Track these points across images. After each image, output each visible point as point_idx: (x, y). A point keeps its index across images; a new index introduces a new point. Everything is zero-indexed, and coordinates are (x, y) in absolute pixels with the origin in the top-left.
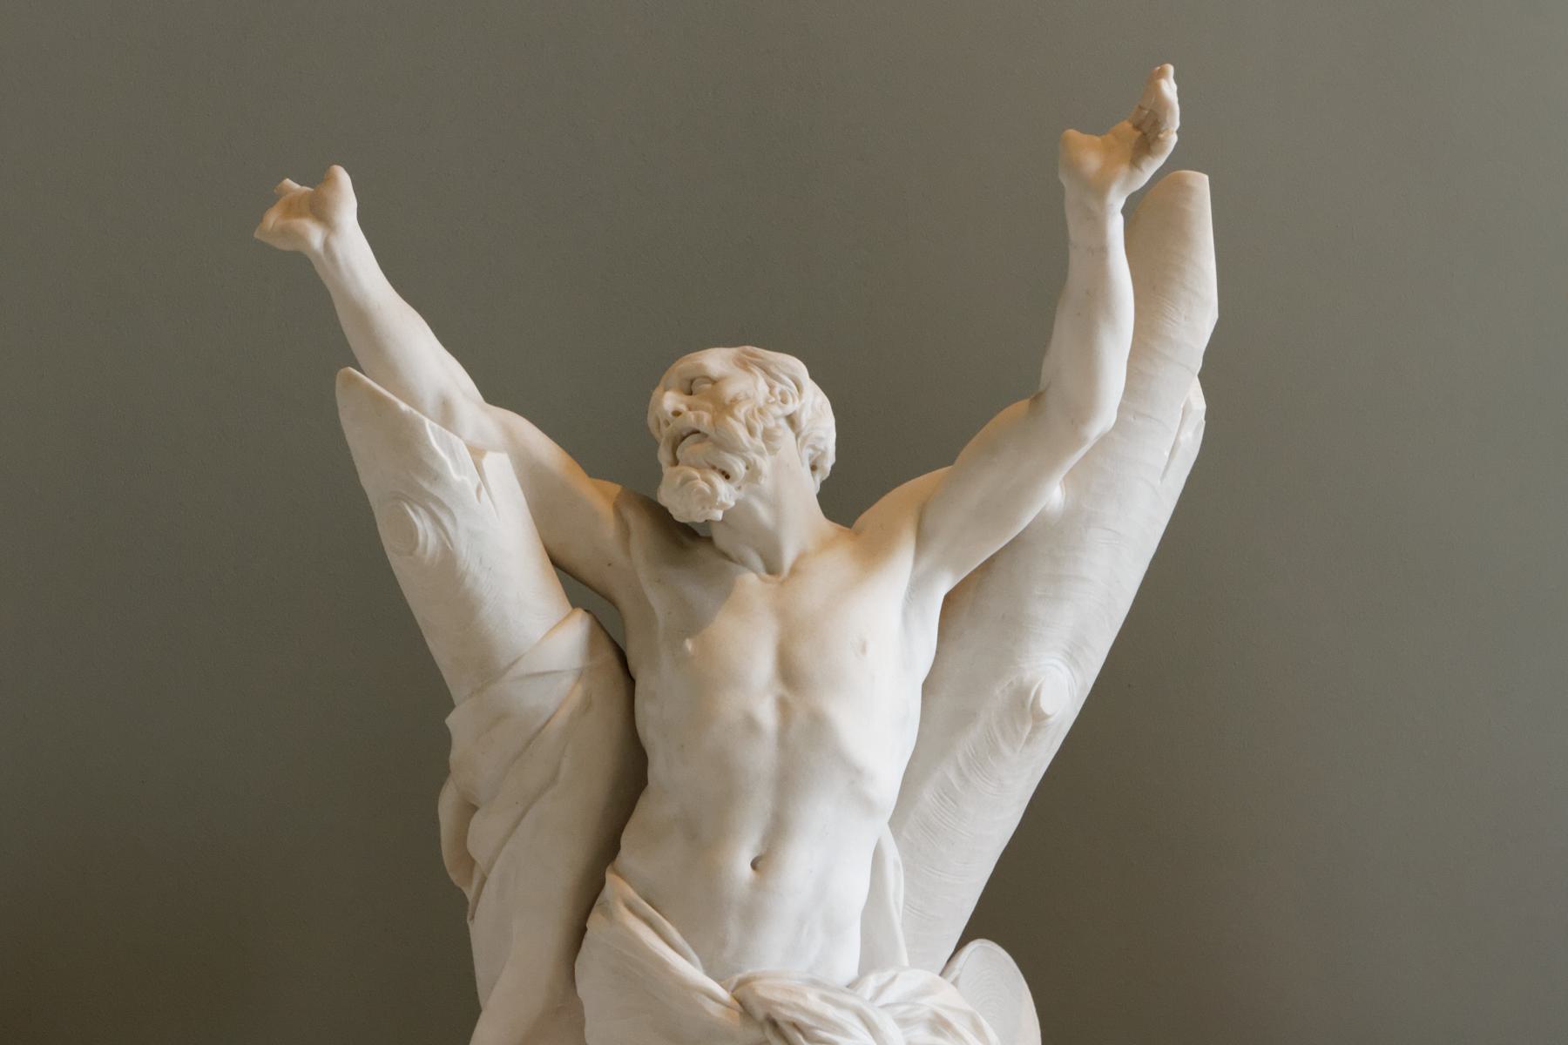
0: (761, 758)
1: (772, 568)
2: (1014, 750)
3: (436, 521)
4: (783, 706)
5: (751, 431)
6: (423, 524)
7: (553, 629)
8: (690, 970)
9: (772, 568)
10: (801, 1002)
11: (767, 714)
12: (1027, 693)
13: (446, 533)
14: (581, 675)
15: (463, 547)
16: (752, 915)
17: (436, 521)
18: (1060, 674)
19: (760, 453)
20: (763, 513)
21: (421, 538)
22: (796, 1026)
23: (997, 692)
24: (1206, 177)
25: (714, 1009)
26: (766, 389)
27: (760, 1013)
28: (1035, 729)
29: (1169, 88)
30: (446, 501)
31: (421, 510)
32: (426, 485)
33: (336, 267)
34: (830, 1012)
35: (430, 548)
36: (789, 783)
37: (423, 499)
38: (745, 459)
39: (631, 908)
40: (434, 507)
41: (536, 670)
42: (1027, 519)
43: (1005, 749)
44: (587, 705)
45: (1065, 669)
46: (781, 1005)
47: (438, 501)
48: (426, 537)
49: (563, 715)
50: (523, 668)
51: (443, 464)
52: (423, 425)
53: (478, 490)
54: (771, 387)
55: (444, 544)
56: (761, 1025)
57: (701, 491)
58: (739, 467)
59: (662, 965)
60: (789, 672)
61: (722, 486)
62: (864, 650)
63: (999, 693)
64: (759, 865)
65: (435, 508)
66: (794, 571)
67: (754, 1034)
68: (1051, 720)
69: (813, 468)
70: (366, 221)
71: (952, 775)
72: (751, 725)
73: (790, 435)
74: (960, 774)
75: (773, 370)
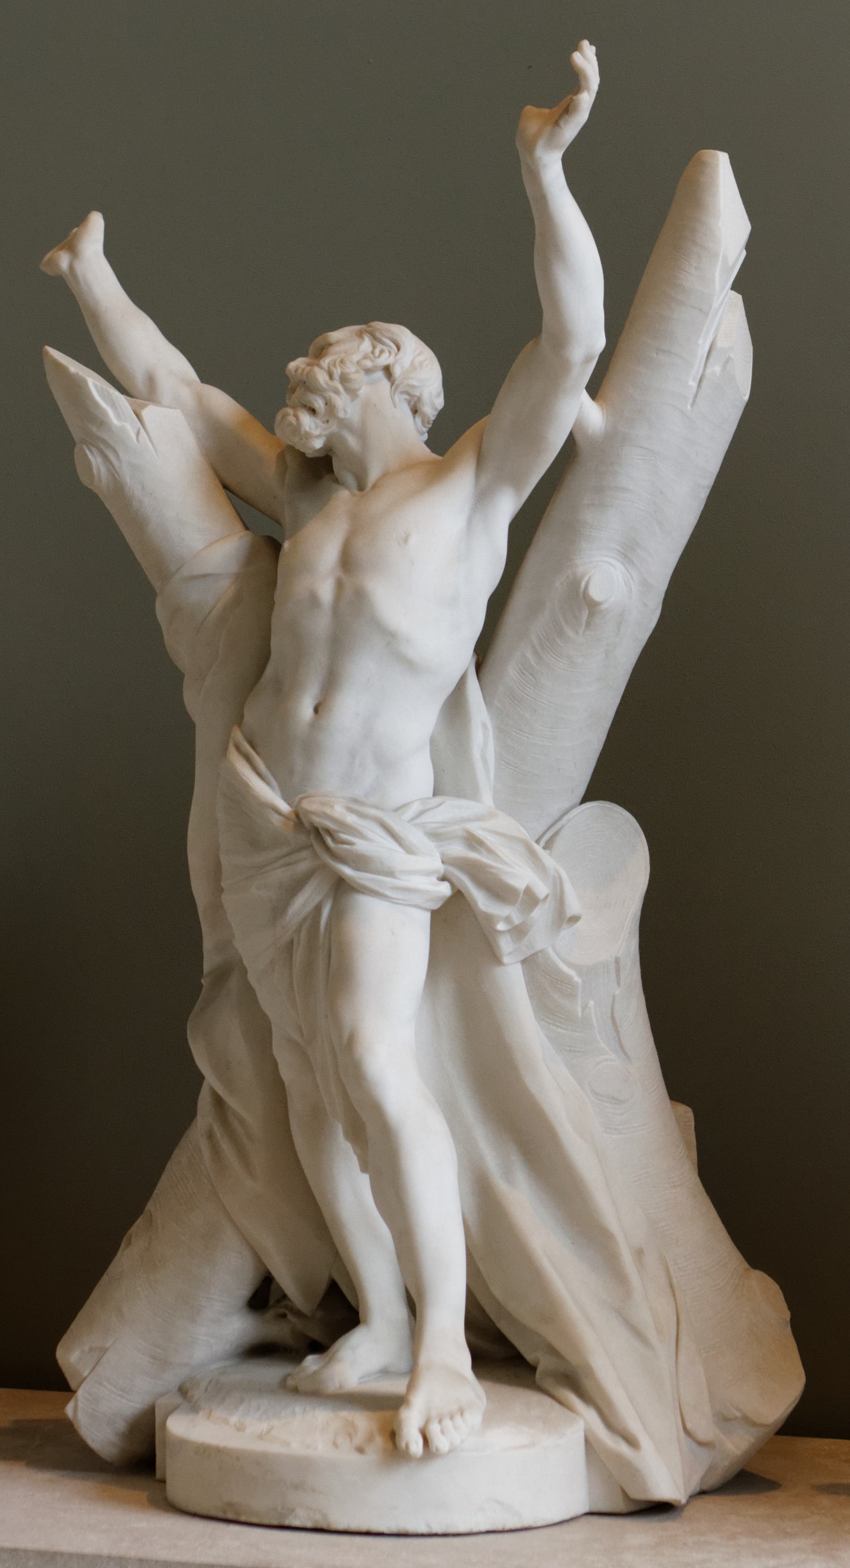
0: (320, 625)
1: (361, 488)
2: (577, 633)
3: (106, 458)
4: (340, 585)
5: (331, 376)
6: (95, 460)
7: (210, 544)
8: (266, 792)
9: (361, 488)
10: (328, 811)
11: (326, 591)
12: (579, 583)
13: (113, 466)
14: (240, 578)
15: (128, 478)
16: (311, 748)
17: (106, 458)
18: (624, 572)
19: (337, 392)
20: (352, 441)
21: (95, 471)
22: (328, 832)
23: (558, 584)
24: (529, 107)
25: (276, 819)
26: (370, 349)
27: (307, 825)
28: (592, 614)
29: (587, 59)
30: (111, 442)
31: (94, 449)
32: (94, 429)
33: (77, 282)
34: (351, 819)
35: (104, 479)
36: (339, 644)
37: (96, 442)
38: (324, 398)
39: (238, 748)
40: (103, 447)
41: (195, 573)
42: (556, 441)
43: (570, 633)
44: (237, 600)
45: (618, 565)
46: (314, 813)
47: (105, 442)
48: (99, 471)
49: (219, 606)
50: (185, 572)
51: (104, 412)
52: (85, 382)
53: (138, 434)
54: (374, 347)
55: (113, 475)
56: (308, 833)
57: (290, 424)
58: (319, 404)
59: (246, 785)
60: (348, 561)
61: (306, 420)
62: (406, 540)
63: (559, 584)
64: (320, 710)
65: (102, 446)
66: (375, 486)
67: (302, 839)
68: (604, 607)
69: (415, 411)
70: (111, 251)
71: (529, 655)
72: (314, 601)
73: (386, 383)
74: (535, 652)
75: (378, 335)
